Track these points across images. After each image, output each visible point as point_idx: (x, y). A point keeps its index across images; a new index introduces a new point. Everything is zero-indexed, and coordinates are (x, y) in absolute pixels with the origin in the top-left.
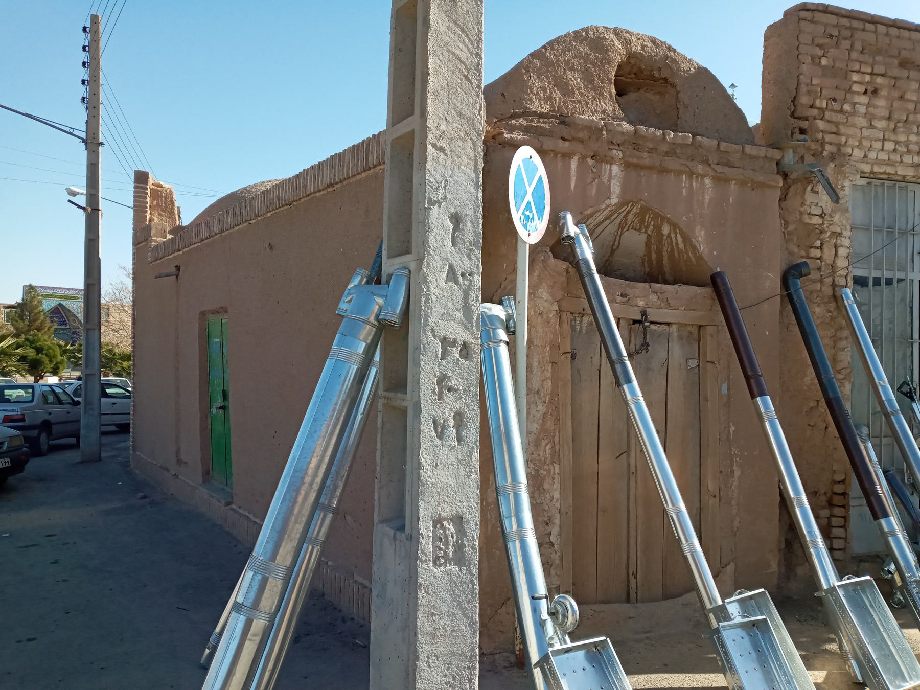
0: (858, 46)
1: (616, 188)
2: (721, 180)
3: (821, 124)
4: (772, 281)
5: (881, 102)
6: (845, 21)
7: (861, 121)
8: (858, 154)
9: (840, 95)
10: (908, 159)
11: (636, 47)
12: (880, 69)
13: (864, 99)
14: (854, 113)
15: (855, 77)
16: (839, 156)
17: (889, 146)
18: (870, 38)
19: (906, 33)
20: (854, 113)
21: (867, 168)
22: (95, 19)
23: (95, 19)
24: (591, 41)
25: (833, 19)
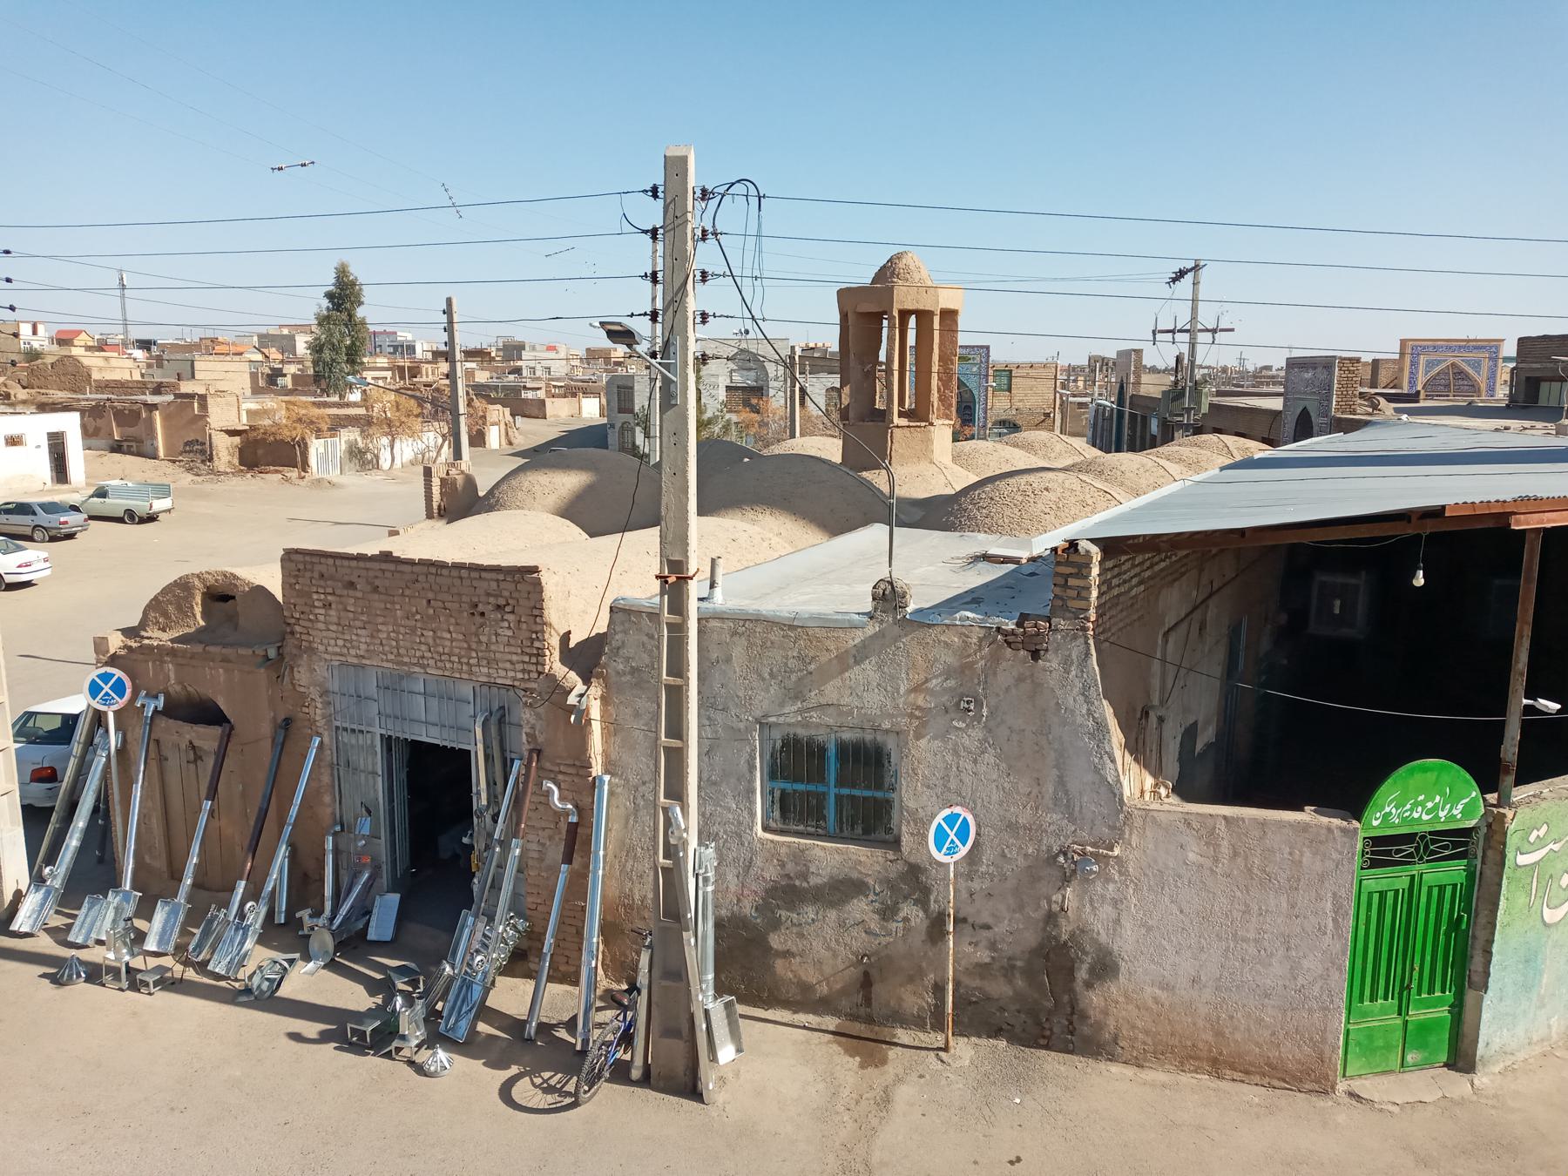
0: (316, 575)
1: (172, 675)
2: (226, 671)
3: (298, 628)
4: (266, 729)
5: (332, 613)
6: (308, 558)
7: (321, 626)
8: (321, 648)
9: (307, 609)
10: (353, 652)
11: (211, 580)
12: (330, 590)
13: (322, 611)
14: (317, 620)
15: (315, 596)
16: (311, 650)
17: (340, 643)
18: (323, 569)
19: (346, 563)
20: (317, 620)
21: (327, 657)
22: (449, 301)
23: (449, 301)
24: (182, 587)
25: (300, 558)
